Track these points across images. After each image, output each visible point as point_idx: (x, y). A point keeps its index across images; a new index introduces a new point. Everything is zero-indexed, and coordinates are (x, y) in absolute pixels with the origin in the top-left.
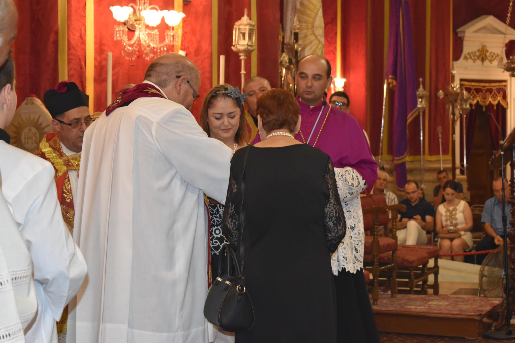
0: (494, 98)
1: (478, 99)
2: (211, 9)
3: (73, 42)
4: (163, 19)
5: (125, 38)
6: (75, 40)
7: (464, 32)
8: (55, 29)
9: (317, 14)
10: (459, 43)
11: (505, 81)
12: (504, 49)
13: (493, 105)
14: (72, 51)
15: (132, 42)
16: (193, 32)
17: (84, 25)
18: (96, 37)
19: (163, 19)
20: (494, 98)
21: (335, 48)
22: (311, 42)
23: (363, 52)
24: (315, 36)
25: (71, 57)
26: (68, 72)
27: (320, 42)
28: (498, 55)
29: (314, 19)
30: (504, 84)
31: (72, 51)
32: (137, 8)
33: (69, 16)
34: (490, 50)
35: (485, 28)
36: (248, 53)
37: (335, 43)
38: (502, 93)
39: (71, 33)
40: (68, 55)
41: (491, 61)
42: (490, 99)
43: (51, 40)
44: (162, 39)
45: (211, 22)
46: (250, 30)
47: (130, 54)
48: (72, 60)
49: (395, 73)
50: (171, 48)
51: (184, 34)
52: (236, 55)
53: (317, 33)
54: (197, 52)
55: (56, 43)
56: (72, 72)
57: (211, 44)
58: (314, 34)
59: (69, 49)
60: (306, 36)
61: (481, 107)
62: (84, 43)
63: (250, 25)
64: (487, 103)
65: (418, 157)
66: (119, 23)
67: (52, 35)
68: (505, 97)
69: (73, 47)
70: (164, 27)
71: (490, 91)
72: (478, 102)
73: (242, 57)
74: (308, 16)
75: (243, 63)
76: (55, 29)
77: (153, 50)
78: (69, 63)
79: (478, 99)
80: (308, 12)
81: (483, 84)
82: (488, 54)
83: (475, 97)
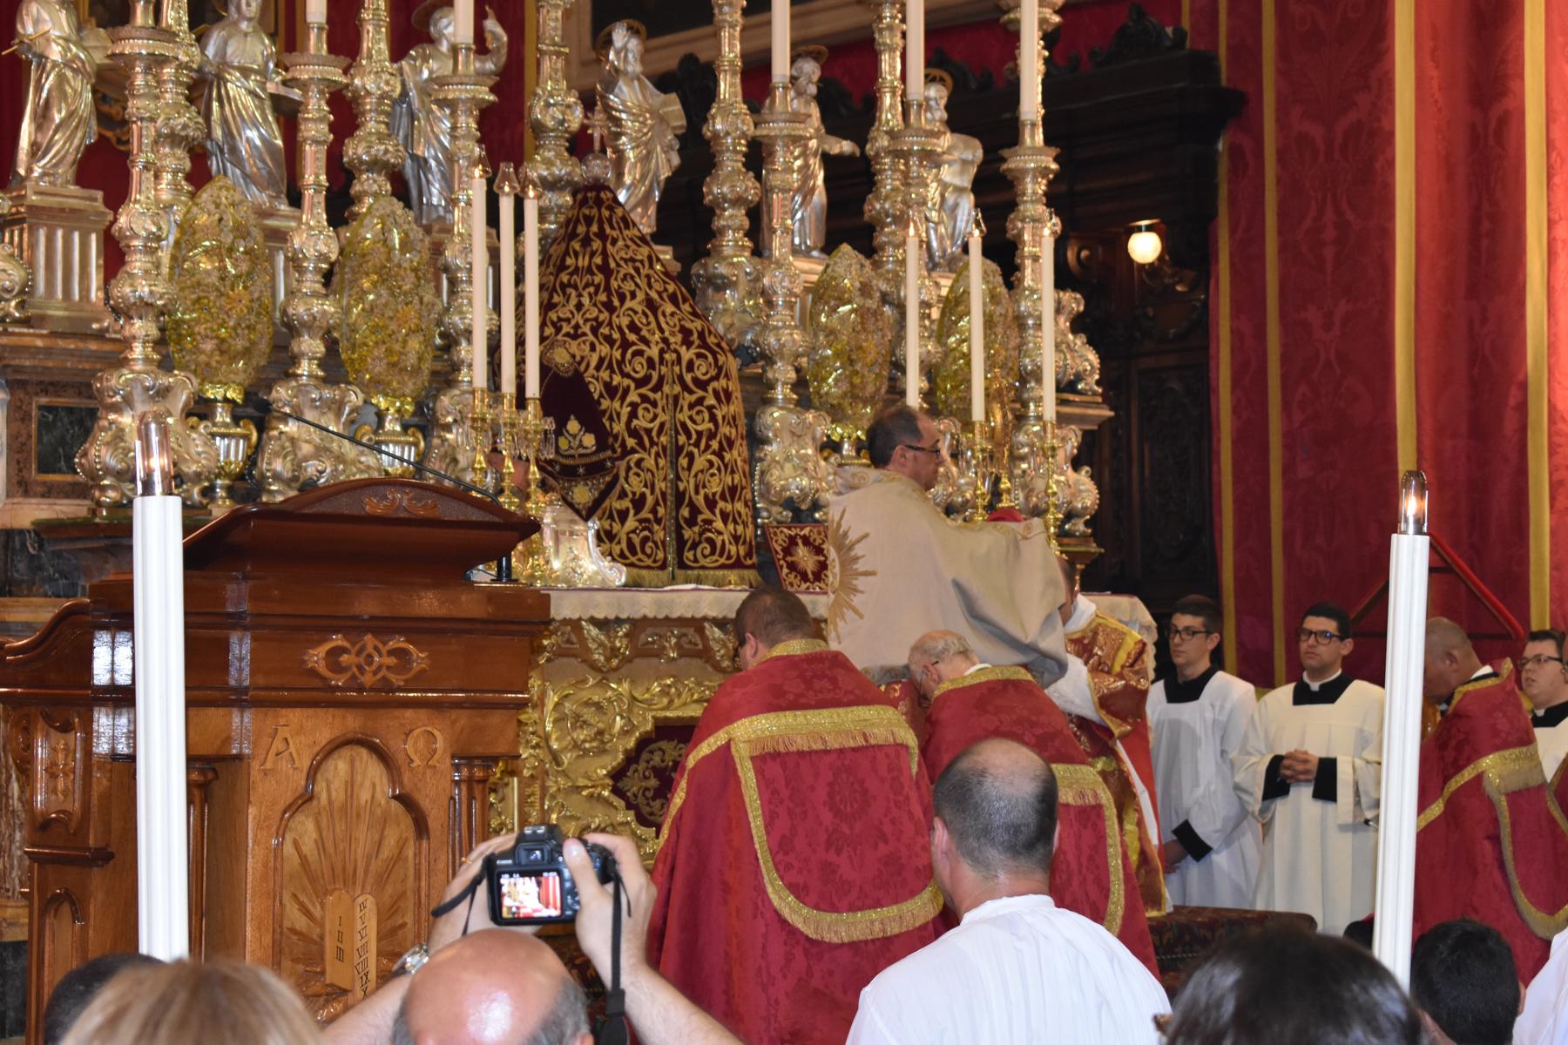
8: (1521, 377)
14: (1561, 426)
25: (1556, 439)
26: (1551, 474)
33: (1552, 347)
39: (1556, 385)
40: (1550, 436)
43: (1512, 402)
48: (1560, 446)
55: (1522, 407)
56: (1558, 476)
59: (1552, 421)
67: (1514, 392)
69: (1563, 418)
76: (1521, 377)
78: (1552, 454)
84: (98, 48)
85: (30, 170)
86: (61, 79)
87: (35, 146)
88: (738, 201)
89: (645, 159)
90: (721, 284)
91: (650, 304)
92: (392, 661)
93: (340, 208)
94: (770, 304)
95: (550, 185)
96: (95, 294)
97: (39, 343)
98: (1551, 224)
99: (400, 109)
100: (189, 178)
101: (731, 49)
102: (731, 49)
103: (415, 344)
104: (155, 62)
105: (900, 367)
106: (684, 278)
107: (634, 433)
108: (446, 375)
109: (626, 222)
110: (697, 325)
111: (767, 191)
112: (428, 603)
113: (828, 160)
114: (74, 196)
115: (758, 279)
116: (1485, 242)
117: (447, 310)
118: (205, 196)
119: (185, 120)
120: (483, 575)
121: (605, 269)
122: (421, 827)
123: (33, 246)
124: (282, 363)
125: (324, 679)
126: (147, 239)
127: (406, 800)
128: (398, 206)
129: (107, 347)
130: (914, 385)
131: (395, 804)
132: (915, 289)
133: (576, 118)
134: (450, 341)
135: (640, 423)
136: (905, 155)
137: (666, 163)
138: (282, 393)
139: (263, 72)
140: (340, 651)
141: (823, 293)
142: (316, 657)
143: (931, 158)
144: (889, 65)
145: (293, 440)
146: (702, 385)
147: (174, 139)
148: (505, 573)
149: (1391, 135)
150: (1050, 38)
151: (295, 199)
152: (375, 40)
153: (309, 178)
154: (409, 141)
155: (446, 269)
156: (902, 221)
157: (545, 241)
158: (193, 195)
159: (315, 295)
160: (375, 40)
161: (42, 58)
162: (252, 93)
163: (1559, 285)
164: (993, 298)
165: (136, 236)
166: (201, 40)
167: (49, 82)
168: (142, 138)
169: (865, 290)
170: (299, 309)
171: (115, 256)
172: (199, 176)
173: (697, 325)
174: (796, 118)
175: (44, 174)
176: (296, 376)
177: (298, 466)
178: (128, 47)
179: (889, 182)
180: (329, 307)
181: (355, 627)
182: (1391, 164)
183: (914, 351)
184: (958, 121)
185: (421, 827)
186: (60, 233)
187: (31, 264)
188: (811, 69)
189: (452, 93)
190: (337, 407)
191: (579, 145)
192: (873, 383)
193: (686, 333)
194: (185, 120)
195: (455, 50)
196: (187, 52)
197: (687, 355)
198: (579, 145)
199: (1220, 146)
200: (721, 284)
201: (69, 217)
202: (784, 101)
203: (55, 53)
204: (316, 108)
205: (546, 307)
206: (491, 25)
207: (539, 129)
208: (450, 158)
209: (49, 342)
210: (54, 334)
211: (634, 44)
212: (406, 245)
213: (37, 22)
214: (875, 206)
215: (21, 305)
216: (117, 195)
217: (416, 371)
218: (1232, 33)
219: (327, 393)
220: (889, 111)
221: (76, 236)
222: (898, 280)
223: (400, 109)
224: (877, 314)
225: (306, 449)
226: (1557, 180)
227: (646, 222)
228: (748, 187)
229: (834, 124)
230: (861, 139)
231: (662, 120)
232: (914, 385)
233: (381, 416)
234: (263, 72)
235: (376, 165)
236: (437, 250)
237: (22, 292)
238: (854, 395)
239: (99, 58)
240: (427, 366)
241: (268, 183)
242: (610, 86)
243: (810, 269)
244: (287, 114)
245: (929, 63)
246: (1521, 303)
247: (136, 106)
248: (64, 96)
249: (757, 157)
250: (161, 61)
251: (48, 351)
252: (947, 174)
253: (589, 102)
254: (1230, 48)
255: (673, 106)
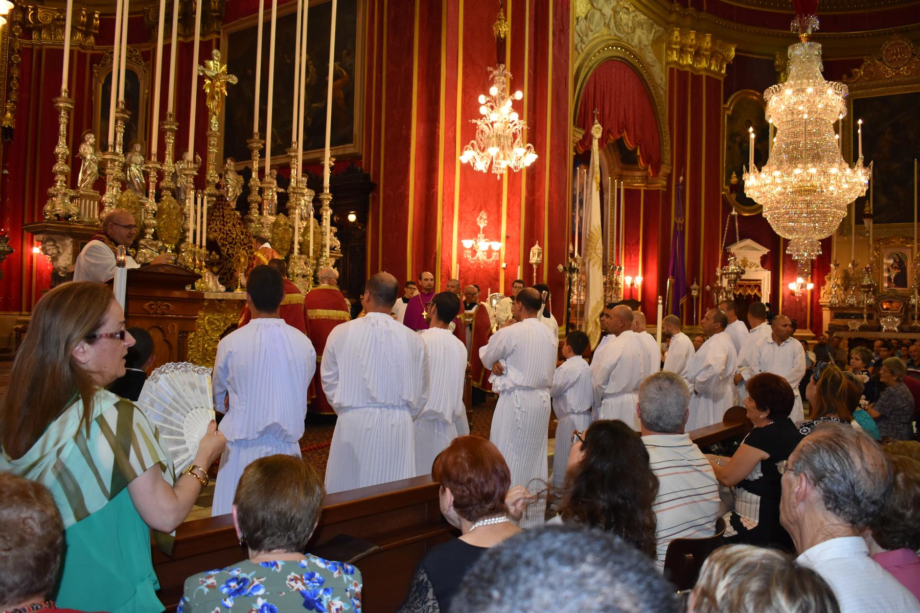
0: (752, 291)
1: (741, 291)
2: (519, 241)
3: (443, 259)
4: (490, 247)
5: (469, 257)
6: (446, 255)
7: (730, 249)
9: (598, 241)
10: (727, 254)
11: (760, 280)
12: (760, 260)
13: (751, 295)
15: (474, 258)
16: (510, 253)
17: (451, 249)
18: (458, 255)
19: (490, 247)
20: (752, 291)
21: (638, 259)
22: (593, 258)
23: (655, 261)
24: (597, 254)
27: (599, 257)
28: (755, 264)
29: (596, 244)
30: (759, 282)
31: (443, 263)
32: (478, 241)
34: (749, 260)
35: (745, 247)
36: (540, 266)
37: (638, 256)
38: (757, 288)
41: (750, 267)
42: (749, 291)
43: (433, 257)
44: (489, 256)
45: (519, 248)
46: (538, 252)
47: (473, 265)
49: (673, 275)
50: (498, 263)
51: (506, 253)
52: (531, 265)
53: (597, 252)
54: (512, 264)
55: (435, 258)
57: (519, 259)
58: (595, 252)
59: (441, 262)
60: (591, 254)
61: (743, 296)
62: (451, 259)
63: (539, 249)
64: (747, 294)
65: (692, 327)
66: (467, 249)
68: (760, 290)
70: (490, 252)
71: (749, 286)
72: (740, 293)
73: (535, 266)
74: (593, 243)
75: (535, 269)
77: (485, 262)
79: (741, 291)
80: (593, 240)
81: (744, 282)
82: (748, 263)
83: (738, 290)
84: (100, 156)
85: (81, 185)
86: (90, 163)
87: (82, 179)
88: (256, 202)
89: (234, 191)
90: (251, 221)
91: (234, 225)
92: (165, 307)
93: (158, 198)
94: (263, 226)
95: (210, 195)
96: (96, 216)
97: (82, 227)
98: (443, 218)
99: (175, 176)
100: (121, 189)
101: (256, 166)
102: (256, 166)
103: (175, 232)
104: (113, 161)
105: (293, 243)
106: (242, 219)
107: (228, 255)
108: (183, 239)
109: (229, 205)
110: (244, 230)
111: (263, 200)
112: (177, 294)
113: (278, 193)
114: (92, 192)
115: (259, 220)
116: (428, 221)
117: (184, 224)
118: (125, 194)
119: (120, 174)
120: (188, 288)
121: (223, 216)
122: (170, 347)
123: (81, 204)
124: (142, 235)
125: (148, 312)
126: (109, 203)
127: (167, 342)
128: (173, 199)
129: (98, 229)
130: (296, 246)
131: (164, 342)
132: (299, 224)
133: (217, 181)
134: (186, 230)
135: (230, 252)
136: (296, 193)
137: (239, 192)
138: (142, 242)
139: (141, 165)
140: (153, 305)
141: (276, 224)
142: (146, 305)
143: (303, 195)
144: (293, 172)
145: (145, 254)
146: (245, 244)
147: (117, 180)
148: (193, 287)
149: (408, 196)
150: (332, 168)
151: (147, 196)
152: (169, 159)
153: (151, 191)
154: (176, 183)
155: (185, 214)
156: (295, 209)
157: (209, 209)
158: (122, 193)
159: (151, 219)
160: (169, 159)
161: (85, 158)
162: (137, 169)
163: (444, 231)
164: (316, 227)
165: (107, 202)
166: (125, 156)
167: (87, 164)
168: (109, 179)
169: (286, 224)
170: (147, 222)
171: (101, 207)
172: (123, 189)
173: (244, 230)
174: (270, 183)
175: (84, 186)
176: (146, 238)
177: (146, 259)
178: (107, 157)
179: (292, 200)
180: (154, 222)
181: (157, 299)
182: (408, 202)
183: (297, 238)
184: (309, 186)
185: (170, 347)
186: (88, 201)
187: (80, 207)
188: (275, 172)
189: (187, 172)
190: (156, 246)
191: (218, 186)
192: (287, 246)
193: (242, 232)
194: (120, 174)
195: (188, 162)
196: (123, 159)
197: (242, 237)
198: (218, 186)
199: (370, 196)
200: (251, 221)
201: (91, 198)
202: (268, 179)
203: (89, 157)
204: (153, 174)
205: (208, 224)
206: (198, 157)
207: (208, 182)
208: (186, 188)
209: (84, 227)
210: (85, 225)
211: (232, 164)
212: (174, 208)
213: (84, 149)
214: (288, 205)
215: (77, 218)
216: (103, 192)
217: (176, 238)
218: (374, 170)
219: (155, 242)
220: (293, 183)
221: (92, 202)
222: (294, 222)
223: (175, 176)
224: (288, 230)
225: (148, 256)
226: (445, 208)
227: (233, 205)
228: (259, 199)
229: (280, 185)
230: (286, 189)
231: (238, 181)
232: (296, 246)
233: (166, 249)
234: (141, 165)
235: (168, 189)
236: (182, 209)
237: (78, 215)
238: (282, 249)
239: (100, 159)
240: (178, 237)
241: (142, 191)
242: (226, 172)
243: (272, 219)
244: (146, 174)
245: (303, 172)
246: (436, 235)
247: (108, 171)
248: (90, 168)
249: (261, 191)
250: (115, 160)
251: (83, 230)
252: (306, 198)
253: (221, 176)
254: (373, 174)
255: (241, 178)
